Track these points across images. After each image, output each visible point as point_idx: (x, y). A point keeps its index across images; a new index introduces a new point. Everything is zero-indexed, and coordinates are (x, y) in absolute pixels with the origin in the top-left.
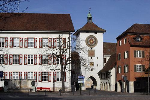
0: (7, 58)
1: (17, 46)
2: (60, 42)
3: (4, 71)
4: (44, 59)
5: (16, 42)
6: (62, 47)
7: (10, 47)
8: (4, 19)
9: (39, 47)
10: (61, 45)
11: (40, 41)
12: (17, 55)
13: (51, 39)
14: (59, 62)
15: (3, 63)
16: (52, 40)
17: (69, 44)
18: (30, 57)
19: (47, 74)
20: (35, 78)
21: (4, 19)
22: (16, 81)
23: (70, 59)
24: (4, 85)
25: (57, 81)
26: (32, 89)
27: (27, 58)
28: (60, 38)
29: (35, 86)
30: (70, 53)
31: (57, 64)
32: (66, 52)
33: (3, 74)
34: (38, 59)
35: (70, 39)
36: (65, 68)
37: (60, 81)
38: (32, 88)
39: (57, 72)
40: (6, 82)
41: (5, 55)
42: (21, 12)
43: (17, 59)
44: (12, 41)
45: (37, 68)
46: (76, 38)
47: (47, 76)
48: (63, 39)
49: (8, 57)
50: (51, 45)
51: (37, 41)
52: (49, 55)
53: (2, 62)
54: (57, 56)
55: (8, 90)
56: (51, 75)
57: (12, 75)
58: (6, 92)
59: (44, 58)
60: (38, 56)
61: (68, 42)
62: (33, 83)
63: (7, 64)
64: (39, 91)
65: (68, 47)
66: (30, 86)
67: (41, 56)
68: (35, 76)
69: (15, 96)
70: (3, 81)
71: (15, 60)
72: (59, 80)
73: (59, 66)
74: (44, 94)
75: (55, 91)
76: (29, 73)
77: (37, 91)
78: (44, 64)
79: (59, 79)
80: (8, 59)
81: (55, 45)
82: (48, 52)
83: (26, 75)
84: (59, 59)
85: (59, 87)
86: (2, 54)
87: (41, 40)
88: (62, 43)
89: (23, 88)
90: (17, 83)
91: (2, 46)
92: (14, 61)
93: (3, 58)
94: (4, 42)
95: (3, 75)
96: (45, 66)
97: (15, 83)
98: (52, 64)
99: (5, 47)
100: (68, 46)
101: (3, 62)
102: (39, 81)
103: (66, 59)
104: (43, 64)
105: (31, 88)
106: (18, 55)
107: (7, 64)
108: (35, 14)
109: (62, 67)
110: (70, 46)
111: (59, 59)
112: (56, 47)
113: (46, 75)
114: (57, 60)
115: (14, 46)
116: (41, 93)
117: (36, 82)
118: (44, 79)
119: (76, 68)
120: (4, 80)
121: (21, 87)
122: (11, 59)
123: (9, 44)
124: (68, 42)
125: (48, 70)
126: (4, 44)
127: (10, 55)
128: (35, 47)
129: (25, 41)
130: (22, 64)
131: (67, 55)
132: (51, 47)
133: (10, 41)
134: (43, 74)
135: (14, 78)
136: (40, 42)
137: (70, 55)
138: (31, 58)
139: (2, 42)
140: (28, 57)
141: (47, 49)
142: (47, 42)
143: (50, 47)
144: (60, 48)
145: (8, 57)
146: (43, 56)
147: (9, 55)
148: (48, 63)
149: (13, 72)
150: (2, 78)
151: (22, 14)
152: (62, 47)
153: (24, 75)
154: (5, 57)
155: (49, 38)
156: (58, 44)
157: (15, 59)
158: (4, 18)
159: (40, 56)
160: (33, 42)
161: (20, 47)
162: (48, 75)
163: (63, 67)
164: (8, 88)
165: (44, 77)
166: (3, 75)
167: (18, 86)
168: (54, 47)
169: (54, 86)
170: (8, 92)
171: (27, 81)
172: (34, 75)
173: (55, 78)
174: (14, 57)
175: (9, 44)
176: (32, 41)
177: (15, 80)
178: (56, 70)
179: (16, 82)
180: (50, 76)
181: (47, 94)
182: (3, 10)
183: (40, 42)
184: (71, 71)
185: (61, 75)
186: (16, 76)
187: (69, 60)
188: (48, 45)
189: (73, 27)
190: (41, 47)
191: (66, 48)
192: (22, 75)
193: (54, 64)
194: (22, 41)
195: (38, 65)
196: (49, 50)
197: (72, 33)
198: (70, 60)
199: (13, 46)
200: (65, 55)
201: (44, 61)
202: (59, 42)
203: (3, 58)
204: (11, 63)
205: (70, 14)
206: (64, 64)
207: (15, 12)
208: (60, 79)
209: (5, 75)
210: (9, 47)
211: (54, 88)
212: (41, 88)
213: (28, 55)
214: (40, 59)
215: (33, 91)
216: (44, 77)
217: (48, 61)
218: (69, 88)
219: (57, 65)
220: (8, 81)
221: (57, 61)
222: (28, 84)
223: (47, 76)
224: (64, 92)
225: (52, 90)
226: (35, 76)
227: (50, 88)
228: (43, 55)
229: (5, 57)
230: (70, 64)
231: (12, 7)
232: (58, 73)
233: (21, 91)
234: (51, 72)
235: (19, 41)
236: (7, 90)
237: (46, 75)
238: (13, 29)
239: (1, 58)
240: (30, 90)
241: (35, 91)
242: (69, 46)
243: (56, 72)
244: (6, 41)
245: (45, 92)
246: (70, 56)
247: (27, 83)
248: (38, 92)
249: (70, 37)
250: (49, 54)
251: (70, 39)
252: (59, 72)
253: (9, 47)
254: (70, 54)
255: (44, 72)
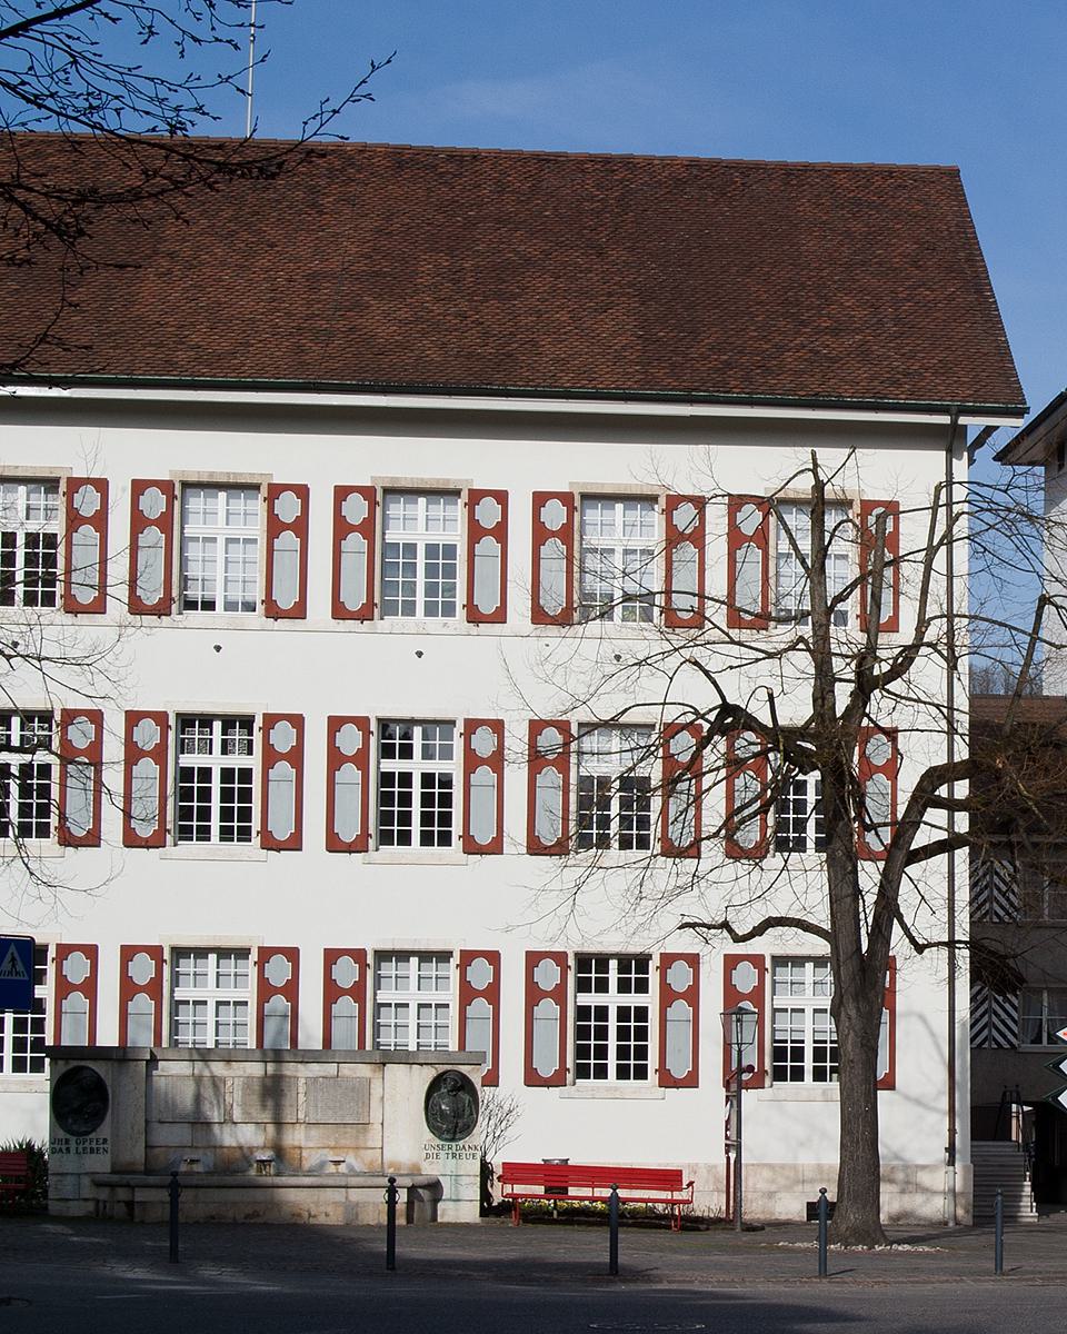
0: (97, 764)
1: (237, 595)
2: (821, 552)
3: (47, 935)
4: (604, 783)
5: (223, 539)
6: (853, 623)
7: (136, 607)
8: (57, 229)
9: (539, 616)
10: (833, 589)
11: (540, 534)
12: (229, 722)
13: (700, 503)
14: (800, 825)
15: (43, 831)
16: (717, 518)
17: (938, 585)
18: (407, 752)
19: (642, 987)
20: (479, 1040)
21: (57, 229)
22: (218, 1068)
23: (962, 789)
24: (45, 1117)
25: (779, 1075)
26: (435, 1187)
27: (361, 760)
28: (818, 504)
29: (478, 1136)
30: (961, 701)
31: (782, 845)
32: (896, 686)
33: (40, 977)
34: (516, 776)
35: (952, 520)
36: (888, 906)
37: (819, 1075)
38: (430, 1170)
39: (780, 961)
40: (83, 1088)
41: (70, 716)
42: (282, 128)
43: (227, 774)
44: (165, 523)
45: (511, 902)
46: (1037, 502)
47: (642, 1013)
48: (868, 506)
49: (113, 750)
50: (701, 596)
51: (500, 532)
52: (671, 730)
53: (25, 810)
54: (777, 736)
55: (112, 1186)
56: (692, 996)
57: (154, 989)
58: (77, 1209)
59: (594, 768)
60: (517, 742)
61: (931, 551)
62: (453, 1105)
63: (93, 839)
64: (535, 1217)
65: (923, 623)
66: (400, 1133)
67: (554, 744)
68: (480, 1006)
69: (209, 1272)
70: (37, 1066)
71: (209, 788)
72: (809, 1063)
73: (801, 884)
74: (590, 1247)
75: (754, 1209)
76: (389, 969)
77: (505, 1209)
78: (604, 842)
79: (798, 1054)
80: (113, 778)
81: (749, 598)
82: (651, 686)
83: (358, 992)
84: (813, 776)
85: (806, 1159)
86: (33, 700)
87: (563, 520)
88: (843, 569)
89: (311, 1159)
90: (235, 1095)
91: (30, 600)
92: (185, 794)
93: (41, 757)
94: (51, 540)
95: (39, 992)
96: (621, 881)
97: (198, 1099)
98: (713, 851)
99: (73, 608)
100: (932, 610)
101: (44, 811)
102: (532, 1078)
103: (908, 780)
104: (584, 842)
105: (415, 1171)
106: (247, 722)
107: (93, 839)
108: (476, 156)
109: (844, 892)
110: (962, 605)
111: (813, 776)
112: (762, 620)
113: (633, 1000)
114: (779, 795)
115: (195, 593)
116: (559, 1232)
117: (485, 1094)
118: (605, 1047)
119: (1032, 904)
120: (58, 1053)
121: (279, 1151)
122: (147, 767)
123: (118, 570)
124: (931, 551)
125: (657, 935)
126: (50, 561)
127: (133, 718)
128: (475, 616)
129: (342, 529)
130: (295, 843)
131: (920, 733)
132: (699, 619)
133: (139, 522)
134: (583, 986)
135: (187, 1036)
136: (553, 548)
137: (951, 731)
138: (417, 766)
139: (32, 540)
140: (387, 752)
141: (642, 638)
142: (638, 543)
143: (682, 620)
144: (822, 636)
145: (113, 750)
146: (590, 743)
147: (115, 724)
148: (654, 831)
149: (180, 953)
150: (19, 1026)
151: (308, 153)
152: (843, 619)
153: (332, 992)
154: (65, 742)
155: (674, 501)
156: (792, 584)
157: (205, 774)
158: (51, 209)
159: (551, 738)
160: (450, 551)
161: (273, 611)
162: (650, 1001)
163: (857, 893)
164: (100, 1163)
165: (605, 1019)
166: (39, 992)
167: (245, 1134)
168: (735, 618)
169: (734, 1145)
170: (99, 1218)
171: (364, 1071)
172: (467, 994)
173: (749, 1031)
174: (182, 747)
175: (118, 570)
176: (441, 538)
177: (204, 1056)
178: (759, 931)
179: (216, 1082)
180: (680, 1009)
181: (636, 1249)
182: (35, 101)
183: (553, 548)
184: (963, 955)
185: (826, 1003)
186: (217, 1004)
187: (939, 803)
188: (657, 585)
189: (1004, 353)
190: (564, 620)
191: (906, 635)
192: (291, 990)
193: (735, 852)
194: (301, 527)
195: (515, 860)
196: (675, 660)
197: (989, 430)
198: (951, 805)
199: (178, 599)
200: (892, 734)
201: (603, 818)
202: (806, 546)
203: (41, 757)
204: (145, 831)
205: (954, 174)
206: (873, 857)
207: (202, 129)
208: (819, 1054)
209: (64, 988)
210: (117, 607)
211: (735, 1172)
212: (557, 1175)
213: (385, 724)
214: (550, 776)
215: (448, 1212)
216: (605, 1019)
217: (656, 803)
218: (939, 1179)
219: (774, 861)
220: (100, 1068)
221: (783, 808)
222: (376, 1117)
223: (642, 1013)
224: (872, 1232)
225: (708, 1201)
226: (480, 1006)
227: (678, 1174)
228: (588, 728)
229: (65, 742)
230: (962, 855)
231: (160, 60)
232: (785, 974)
233: (276, 1205)
234: (693, 960)
235: (258, 529)
236: (88, 1191)
237: (633, 1000)
238: (182, 356)
239: (15, 760)
240: (402, 1196)
241: (469, 1212)
242: (950, 616)
243: (757, 960)
244: (74, 520)
245: (614, 1219)
246: (962, 752)
247: (361, 1093)
248: (511, 1221)
249: (960, 493)
250: (671, 714)
251: (952, 520)
252: (799, 961)
253: (117, 607)
254: (963, 722)
255: (602, 961)
